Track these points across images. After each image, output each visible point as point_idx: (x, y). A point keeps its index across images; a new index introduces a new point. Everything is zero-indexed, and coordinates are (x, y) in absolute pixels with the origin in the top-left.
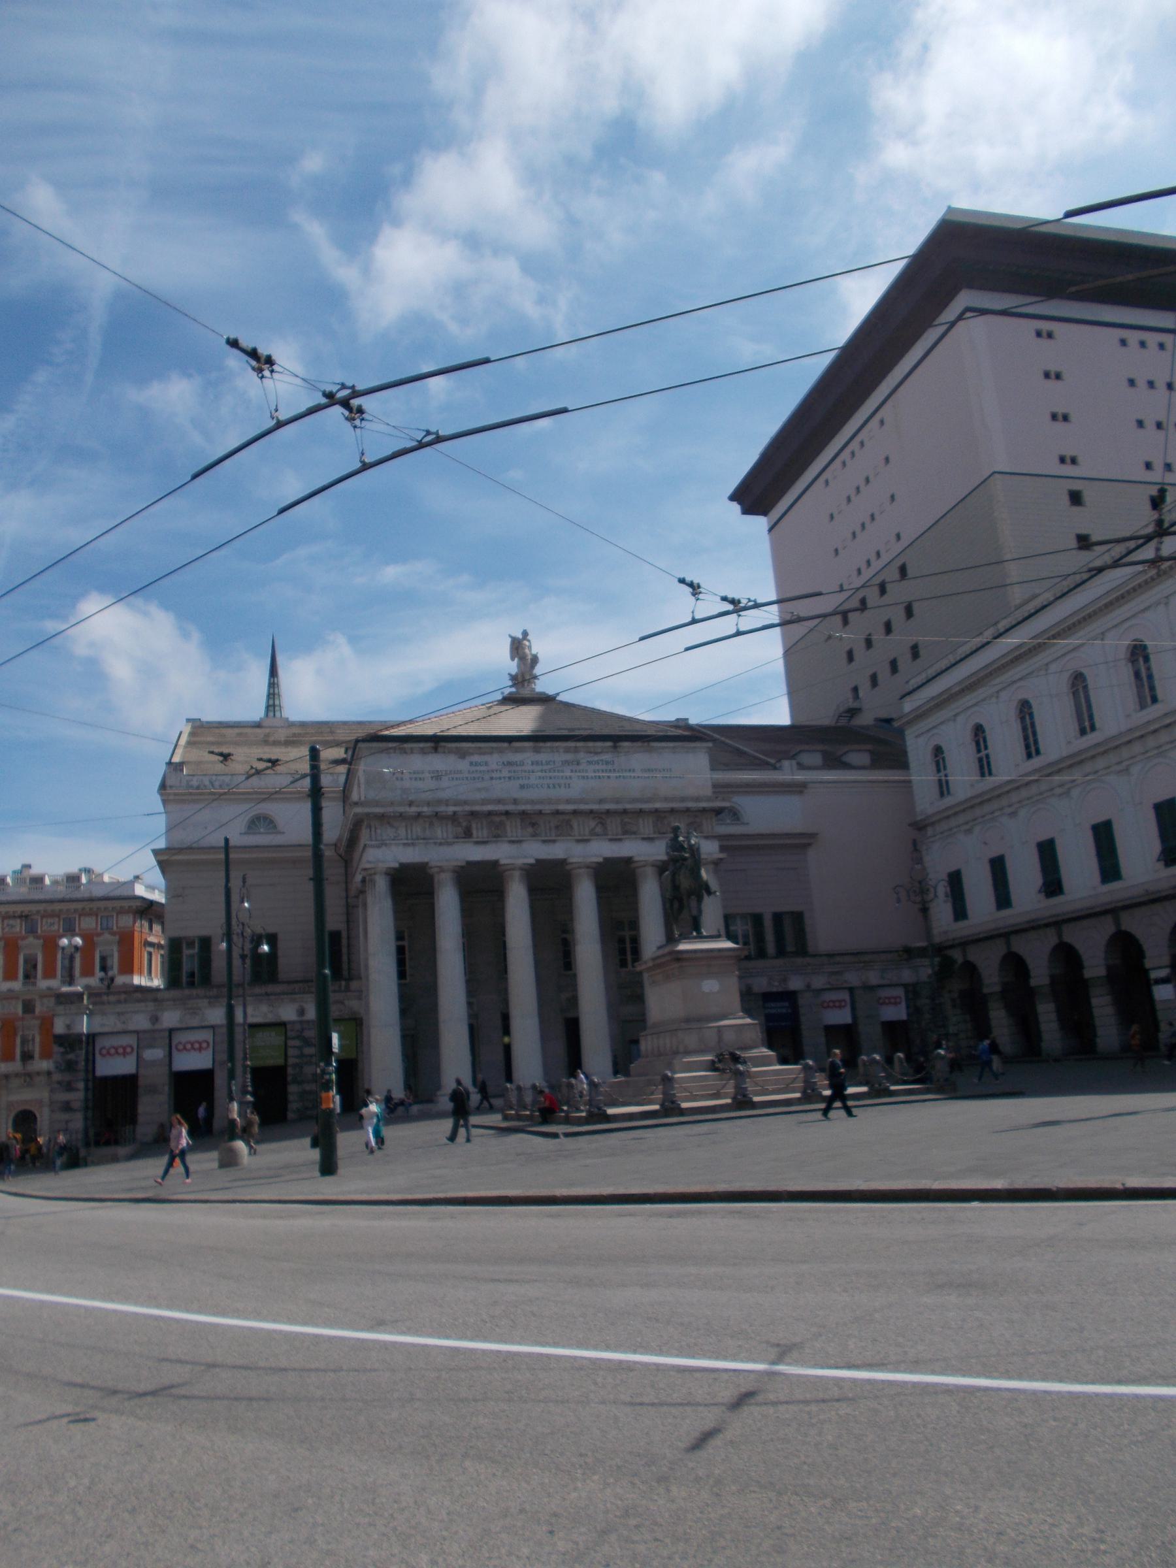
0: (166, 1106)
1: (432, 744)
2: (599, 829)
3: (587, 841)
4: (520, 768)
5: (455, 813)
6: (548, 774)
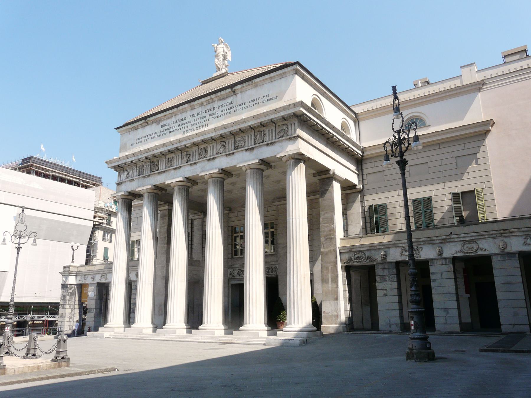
0: (93, 319)
1: (144, 121)
2: (222, 150)
4: (185, 121)
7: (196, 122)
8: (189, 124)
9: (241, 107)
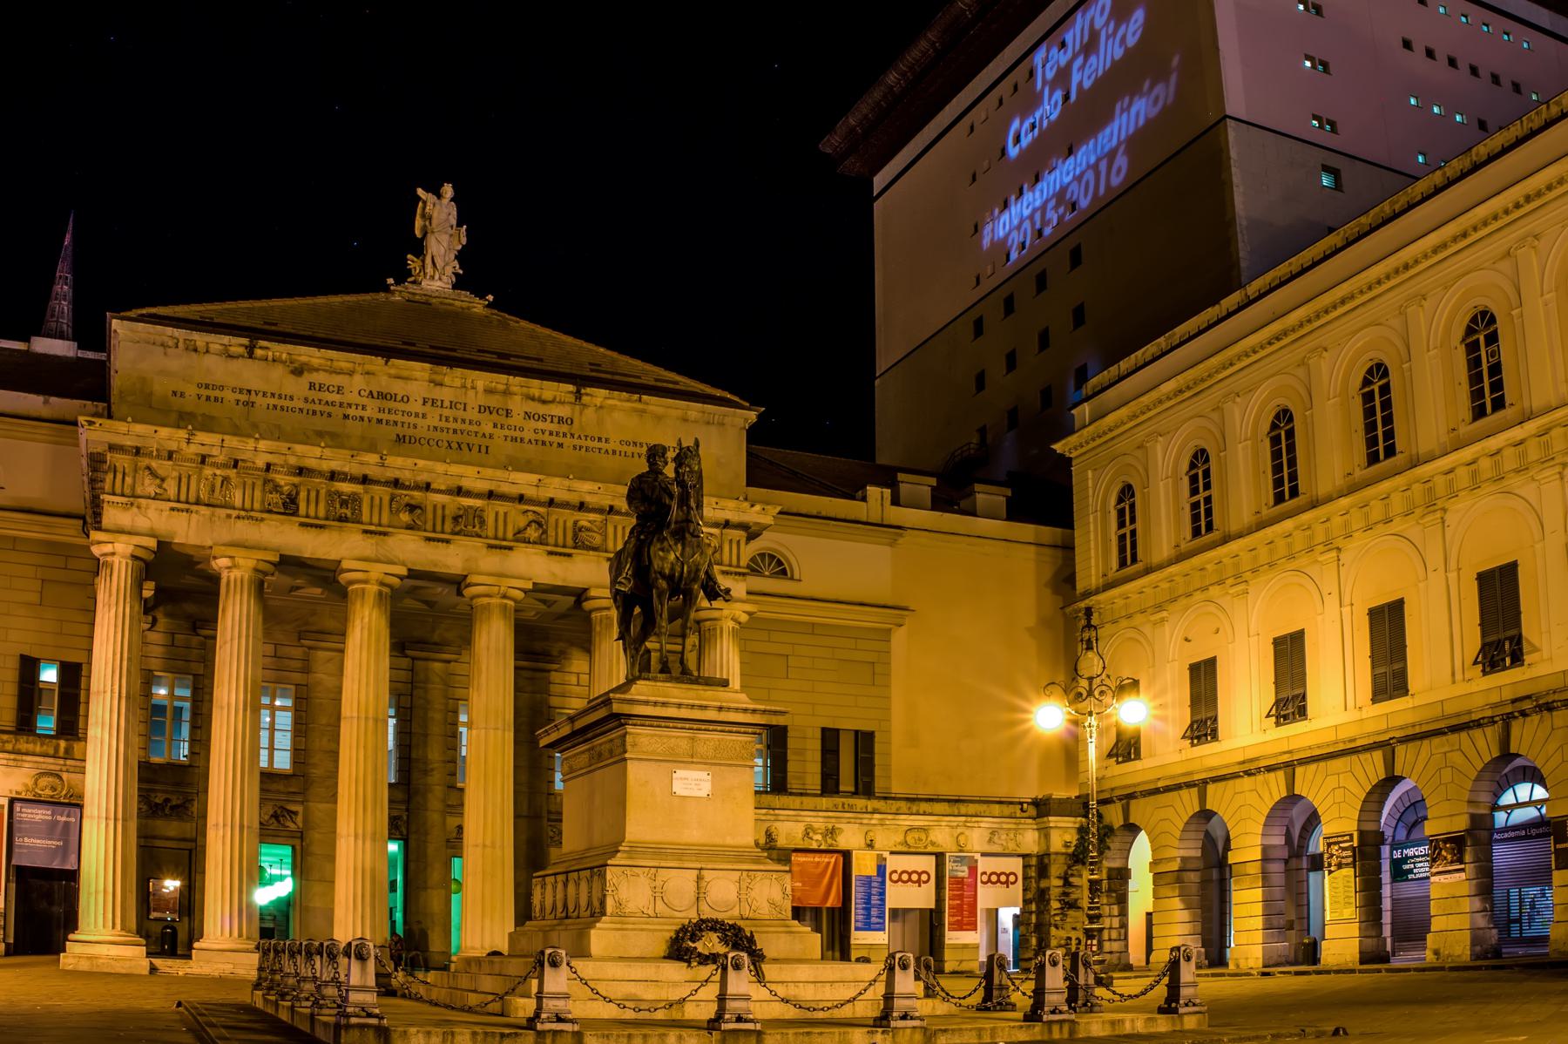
1: (245, 341)
3: (510, 548)
4: (401, 406)
5: (268, 466)
6: (453, 425)
7: (443, 424)
8: (419, 421)
9: (596, 444)
